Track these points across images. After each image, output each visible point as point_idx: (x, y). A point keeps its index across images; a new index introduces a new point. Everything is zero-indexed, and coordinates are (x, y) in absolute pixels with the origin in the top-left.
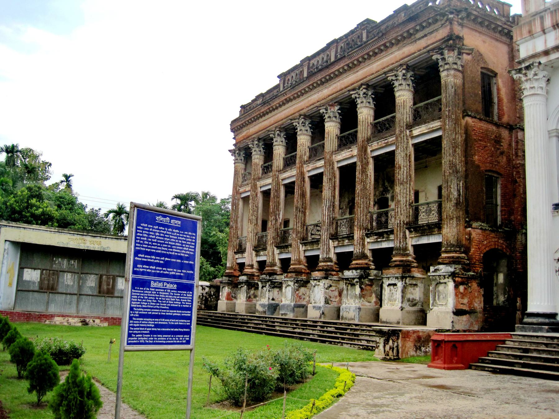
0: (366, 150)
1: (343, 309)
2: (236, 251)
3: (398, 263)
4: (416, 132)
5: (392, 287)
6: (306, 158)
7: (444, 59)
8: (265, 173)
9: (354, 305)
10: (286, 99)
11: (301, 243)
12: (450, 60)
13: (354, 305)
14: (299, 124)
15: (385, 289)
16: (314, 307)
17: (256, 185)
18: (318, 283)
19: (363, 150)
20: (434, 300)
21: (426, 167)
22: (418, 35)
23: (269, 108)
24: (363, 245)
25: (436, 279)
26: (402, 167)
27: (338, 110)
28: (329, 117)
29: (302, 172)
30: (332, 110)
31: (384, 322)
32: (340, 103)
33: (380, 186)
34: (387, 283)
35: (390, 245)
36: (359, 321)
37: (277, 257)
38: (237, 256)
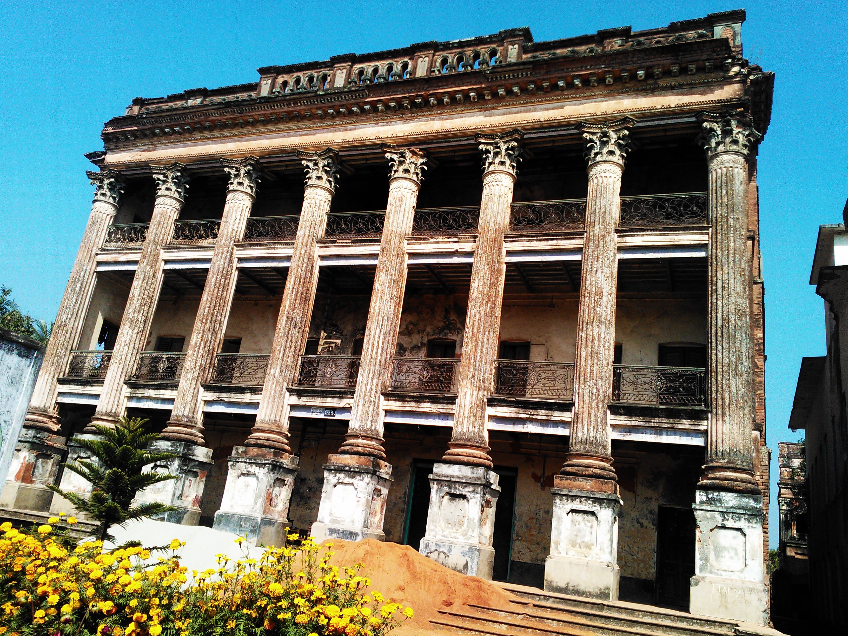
1: (427, 545)
2: (61, 376)
3: (598, 471)
5: (579, 517)
8: (186, 237)
9: (461, 540)
10: (288, 113)
11: (288, 390)
13: (461, 540)
14: (316, 164)
15: (559, 519)
17: (159, 254)
18: (347, 480)
21: (552, 305)
22: (662, 83)
23: (235, 119)
25: (713, 518)
26: (605, 294)
27: (422, 164)
29: (309, 255)
30: (413, 160)
32: (427, 154)
33: (438, 318)
37: (202, 408)
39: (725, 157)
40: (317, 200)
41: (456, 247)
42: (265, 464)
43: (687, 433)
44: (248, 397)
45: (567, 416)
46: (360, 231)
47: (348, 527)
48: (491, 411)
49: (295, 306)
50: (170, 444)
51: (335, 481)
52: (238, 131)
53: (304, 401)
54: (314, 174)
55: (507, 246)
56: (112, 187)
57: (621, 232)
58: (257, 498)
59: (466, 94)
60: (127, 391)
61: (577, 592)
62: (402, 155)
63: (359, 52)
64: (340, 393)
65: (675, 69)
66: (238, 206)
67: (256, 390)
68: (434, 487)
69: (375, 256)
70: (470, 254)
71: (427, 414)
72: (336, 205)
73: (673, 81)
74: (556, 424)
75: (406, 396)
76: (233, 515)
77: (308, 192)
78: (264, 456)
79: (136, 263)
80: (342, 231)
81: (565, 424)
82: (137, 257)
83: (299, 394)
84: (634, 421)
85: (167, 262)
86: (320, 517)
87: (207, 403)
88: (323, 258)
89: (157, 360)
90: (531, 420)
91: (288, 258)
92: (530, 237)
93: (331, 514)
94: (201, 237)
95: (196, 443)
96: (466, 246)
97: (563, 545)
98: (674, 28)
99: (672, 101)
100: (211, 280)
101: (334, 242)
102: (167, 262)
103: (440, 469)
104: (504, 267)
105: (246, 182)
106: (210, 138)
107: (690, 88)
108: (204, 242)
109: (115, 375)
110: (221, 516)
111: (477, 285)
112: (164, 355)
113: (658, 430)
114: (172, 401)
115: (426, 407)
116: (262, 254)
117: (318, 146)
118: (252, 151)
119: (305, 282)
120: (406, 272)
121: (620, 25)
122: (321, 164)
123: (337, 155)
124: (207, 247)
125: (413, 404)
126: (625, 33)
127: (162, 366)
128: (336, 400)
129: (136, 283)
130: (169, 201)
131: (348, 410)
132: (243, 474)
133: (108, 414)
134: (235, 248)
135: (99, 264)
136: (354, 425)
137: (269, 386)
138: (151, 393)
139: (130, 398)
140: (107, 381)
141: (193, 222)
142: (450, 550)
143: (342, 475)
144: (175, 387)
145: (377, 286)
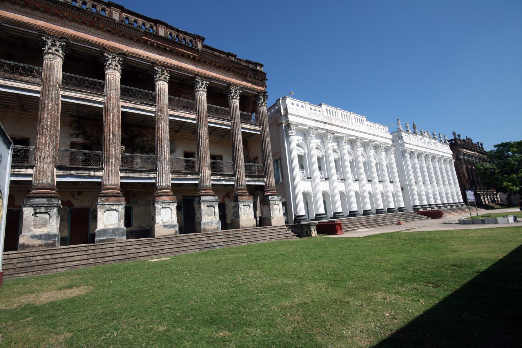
1: (204, 224)
5: (245, 207)
9: (214, 220)
15: (241, 208)
22: (249, 79)
31: (244, 228)
41: (189, 116)
42: (122, 204)
43: (261, 182)
47: (170, 223)
48: (212, 177)
50: (45, 200)
51: (161, 207)
53: (128, 175)
59: (189, 56)
63: (127, 7)
64: (149, 171)
65: (253, 76)
71: (190, 180)
73: (251, 80)
75: (180, 172)
76: (108, 229)
83: (126, 171)
86: (157, 222)
87: (58, 176)
90: (223, 180)
93: (162, 220)
97: (243, 215)
98: (247, 61)
99: (249, 85)
101: (131, 101)
106: (21, 11)
107: (255, 84)
110: (99, 231)
113: (255, 181)
115: (189, 176)
121: (235, 53)
122: (117, 59)
124: (27, 82)
125: (183, 176)
126: (235, 56)
128: (147, 174)
132: (107, 210)
134: (60, 89)
142: (212, 224)
143: (164, 205)
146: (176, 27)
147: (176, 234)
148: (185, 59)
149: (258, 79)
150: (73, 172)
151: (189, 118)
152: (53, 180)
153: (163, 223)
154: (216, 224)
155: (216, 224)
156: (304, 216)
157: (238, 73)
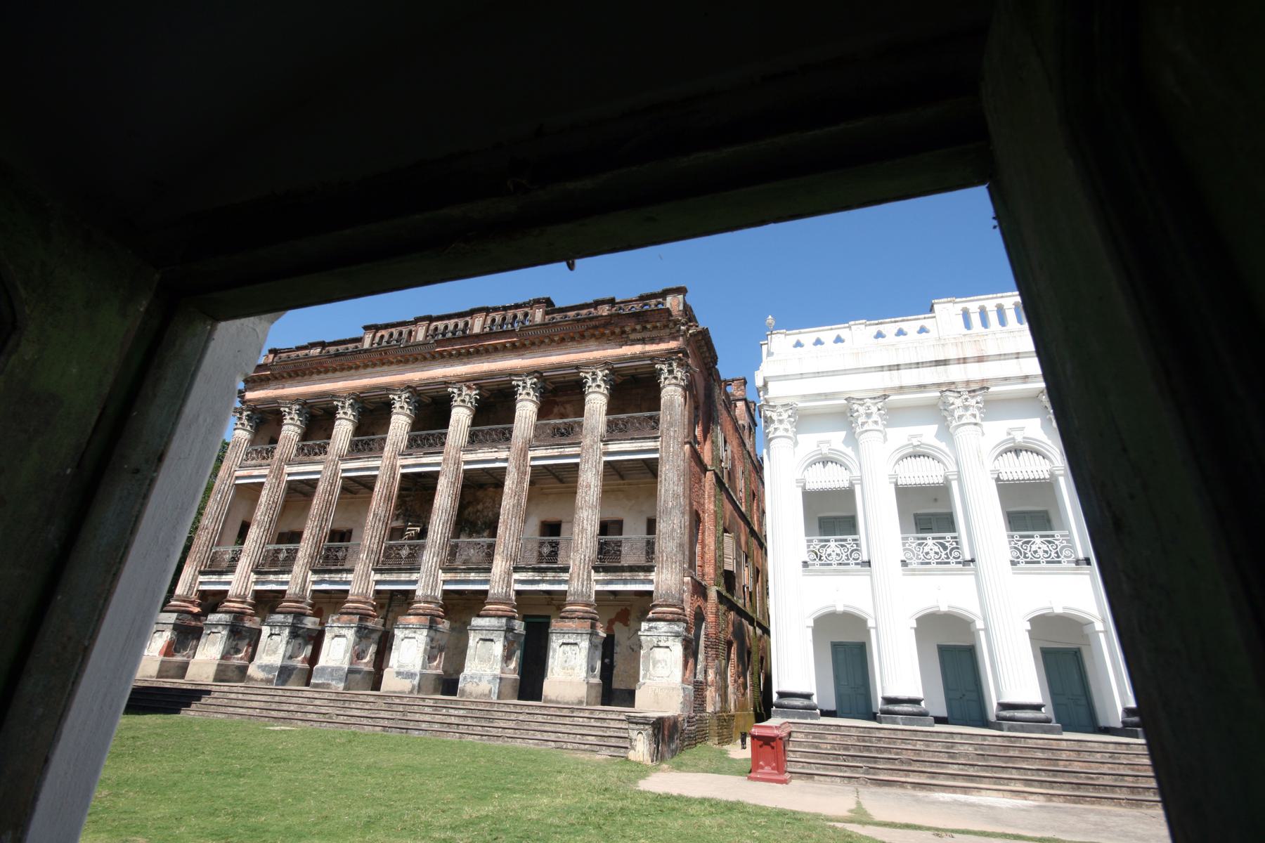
0: (525, 455)
4: (613, 447)
5: (567, 648)
6: (403, 446)
7: (671, 372)
9: (489, 672)
12: (679, 375)
13: (489, 672)
15: (555, 651)
16: (398, 674)
18: (412, 635)
19: (523, 453)
20: (647, 670)
22: (633, 336)
24: (509, 585)
28: (463, 401)
31: (551, 701)
32: (479, 387)
34: (561, 641)
35: (563, 587)
36: (499, 698)
38: (201, 578)
39: (669, 388)
40: (400, 423)
43: (643, 582)
44: (344, 576)
45: (565, 576)
46: (431, 445)
48: (516, 576)
49: (379, 505)
52: (345, 373)
54: (397, 405)
55: (531, 454)
56: (249, 418)
57: (606, 442)
58: (346, 652)
59: (504, 345)
60: (253, 577)
61: (558, 702)
62: (460, 390)
63: (434, 314)
66: (343, 429)
67: (350, 571)
68: (472, 635)
69: (438, 464)
70: (506, 460)
72: (415, 426)
74: (560, 582)
76: (327, 668)
77: (394, 418)
78: (351, 622)
79: (264, 476)
80: (418, 446)
81: (566, 582)
82: (266, 472)
84: (609, 577)
85: (289, 475)
88: (404, 467)
89: (278, 551)
91: (377, 468)
92: (547, 446)
94: (316, 454)
95: (304, 615)
96: (503, 455)
98: (642, 298)
99: (637, 349)
100: (321, 487)
102: (289, 475)
103: (476, 622)
104: (529, 469)
105: (349, 411)
108: (318, 458)
109: (244, 564)
111: (509, 484)
112: (284, 547)
113: (625, 582)
114: (286, 583)
115: (472, 576)
116: (358, 466)
117: (402, 383)
118: (355, 388)
119: (389, 486)
120: (461, 475)
121: (607, 296)
123: (414, 388)
126: (612, 302)
127: (282, 556)
129: (264, 493)
130: (292, 428)
131: (415, 582)
133: (236, 596)
135: (237, 478)
136: (419, 593)
137: (359, 568)
138: (272, 577)
139: (256, 583)
140: (238, 570)
141: (310, 443)
144: (289, 572)
145: (439, 487)
146: (500, 304)
147: (411, 692)
148: (500, 355)
149: (655, 328)
150: (327, 576)
151: (496, 460)
152: (303, 589)
153: (400, 666)
154: (489, 682)
155: (489, 682)
156: (1037, 708)
157: (603, 335)
